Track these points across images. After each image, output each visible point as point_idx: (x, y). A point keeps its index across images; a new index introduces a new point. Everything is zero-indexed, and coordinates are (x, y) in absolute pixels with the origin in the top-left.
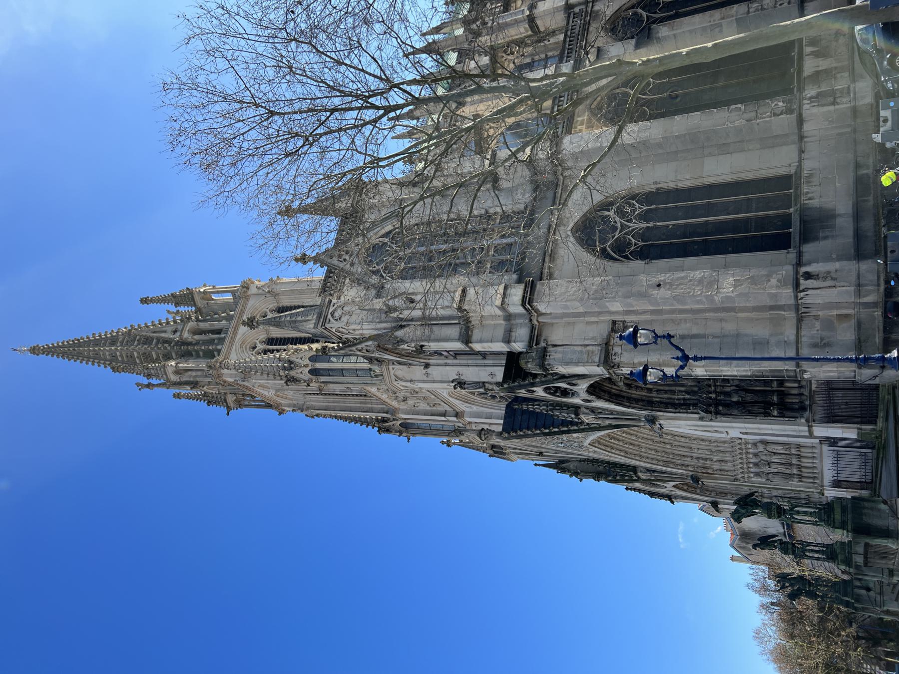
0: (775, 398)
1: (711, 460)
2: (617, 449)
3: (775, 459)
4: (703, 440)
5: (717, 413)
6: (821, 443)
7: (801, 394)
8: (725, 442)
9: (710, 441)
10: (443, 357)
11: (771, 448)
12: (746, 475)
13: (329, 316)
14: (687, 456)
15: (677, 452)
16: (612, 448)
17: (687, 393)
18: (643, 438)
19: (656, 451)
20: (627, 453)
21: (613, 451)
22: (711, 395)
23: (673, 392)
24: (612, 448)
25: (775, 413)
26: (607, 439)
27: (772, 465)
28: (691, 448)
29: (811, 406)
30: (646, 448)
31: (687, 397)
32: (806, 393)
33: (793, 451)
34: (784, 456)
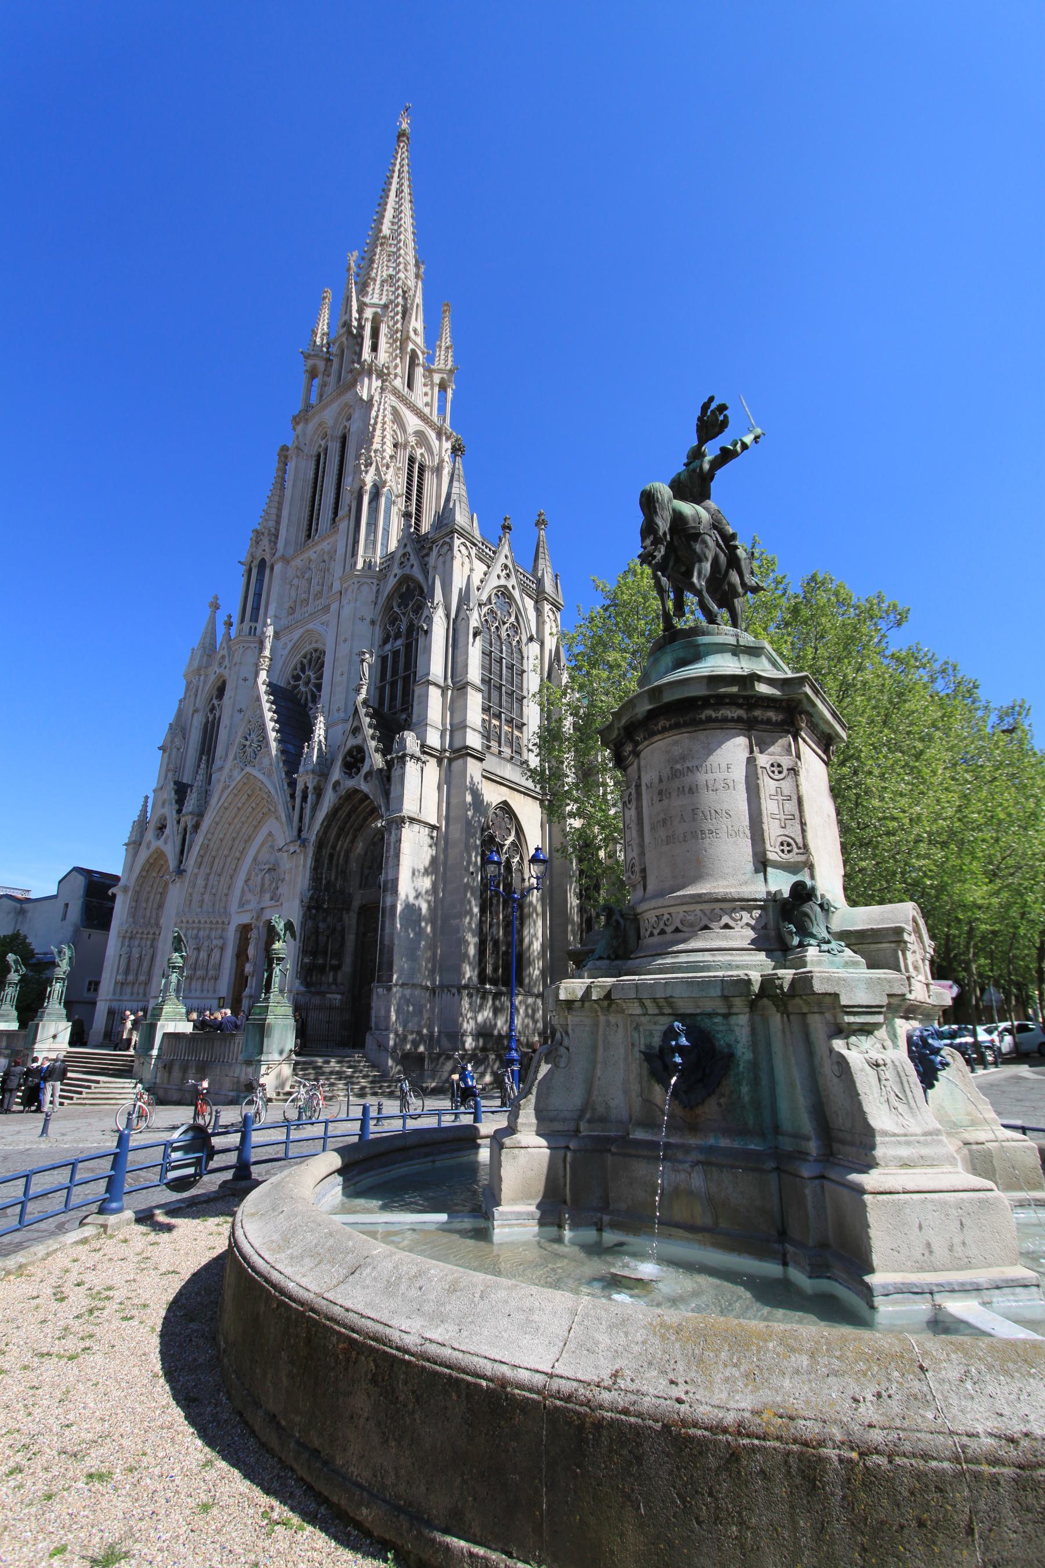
0: (320, 961)
3: (203, 955)
5: (309, 908)
6: (220, 998)
7: (321, 984)
9: (226, 895)
10: (381, 643)
11: (216, 954)
12: (184, 925)
13: (463, 540)
14: (211, 868)
15: (217, 861)
17: (328, 882)
18: (241, 828)
20: (226, 809)
23: (329, 869)
25: (306, 960)
27: (196, 952)
29: (310, 992)
31: (324, 882)
32: (323, 989)
33: (211, 973)
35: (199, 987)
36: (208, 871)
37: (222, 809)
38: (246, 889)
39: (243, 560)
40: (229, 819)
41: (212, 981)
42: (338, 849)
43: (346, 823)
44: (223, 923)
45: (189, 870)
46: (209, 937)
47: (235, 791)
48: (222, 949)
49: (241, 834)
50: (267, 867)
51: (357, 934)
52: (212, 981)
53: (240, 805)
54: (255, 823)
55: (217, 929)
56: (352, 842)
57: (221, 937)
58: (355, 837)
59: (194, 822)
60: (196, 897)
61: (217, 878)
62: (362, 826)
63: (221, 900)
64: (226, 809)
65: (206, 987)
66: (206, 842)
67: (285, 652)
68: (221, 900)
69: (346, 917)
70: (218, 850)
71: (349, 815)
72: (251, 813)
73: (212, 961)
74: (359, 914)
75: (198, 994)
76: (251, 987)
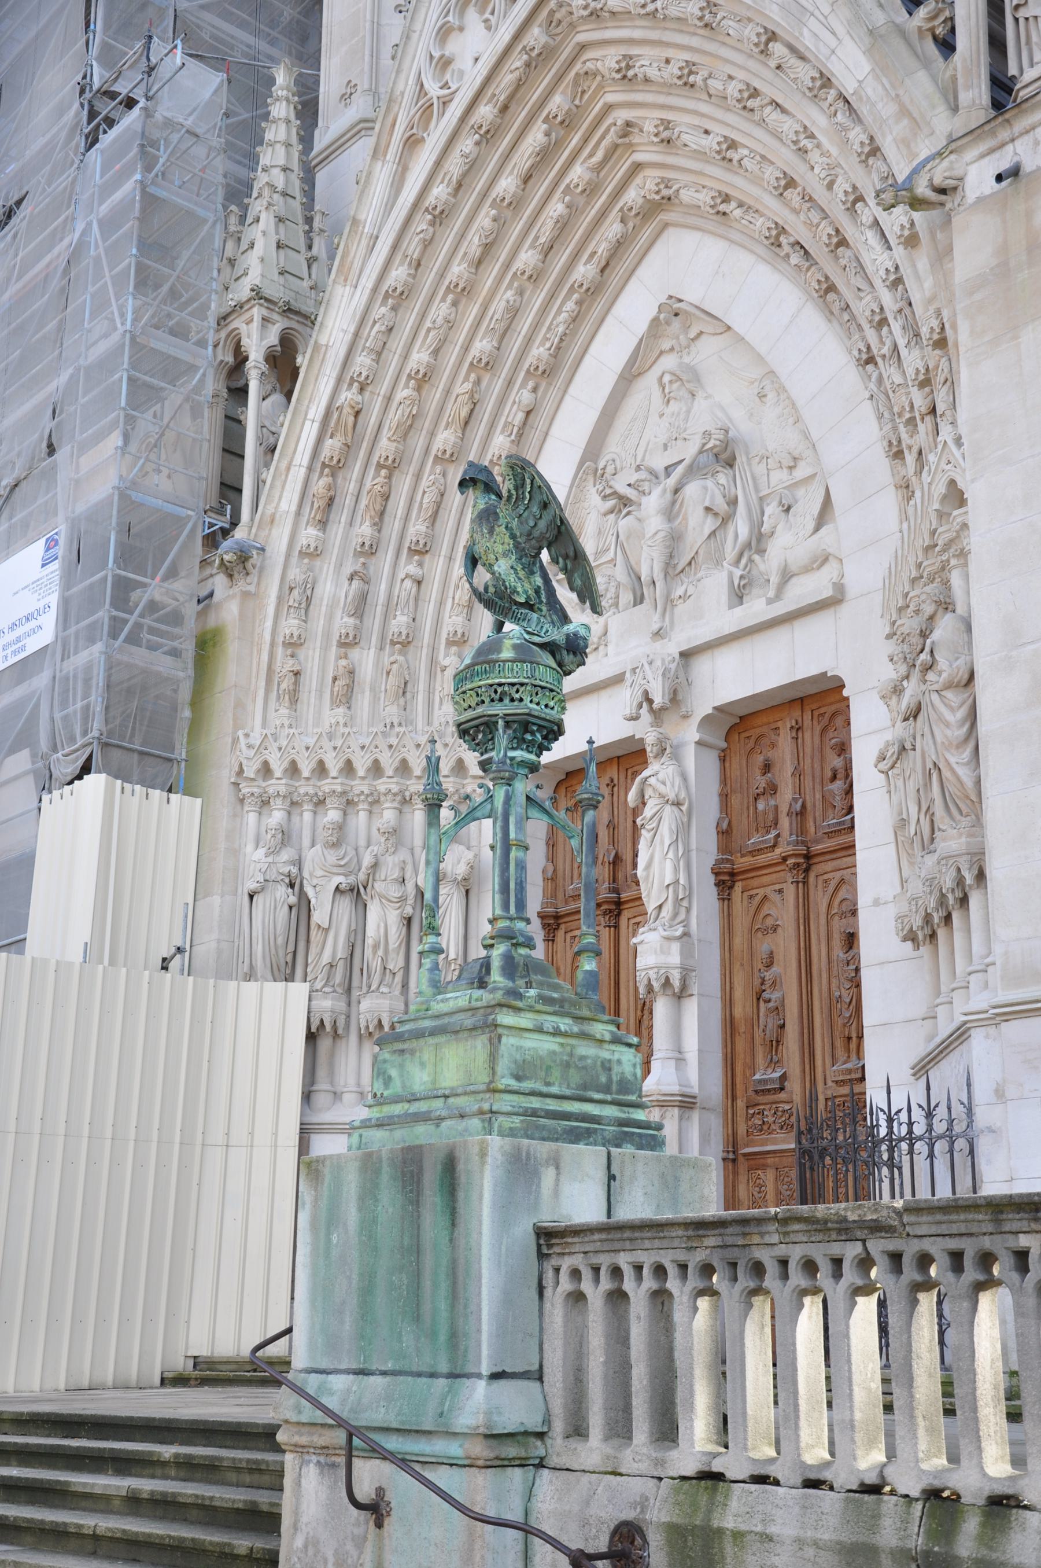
1: (348, 643)
2: (472, 166)
12: (277, 785)
15: (403, 485)
16: (488, 136)
18: (514, 313)
19: (423, 380)
20: (440, 217)
21: (467, 144)
26: (558, 102)
27: (345, 904)
28: (421, 551)
30: (450, 324)
36: (365, 530)
37: (422, 224)
40: (458, 270)
45: (278, 541)
47: (486, 112)
49: (515, 344)
50: (689, 451)
53: (507, 184)
54: (584, 271)
59: (273, 338)
61: (412, 569)
64: (440, 217)
66: (348, 396)
70: (406, 431)
72: (563, 226)
76: (680, 1060)
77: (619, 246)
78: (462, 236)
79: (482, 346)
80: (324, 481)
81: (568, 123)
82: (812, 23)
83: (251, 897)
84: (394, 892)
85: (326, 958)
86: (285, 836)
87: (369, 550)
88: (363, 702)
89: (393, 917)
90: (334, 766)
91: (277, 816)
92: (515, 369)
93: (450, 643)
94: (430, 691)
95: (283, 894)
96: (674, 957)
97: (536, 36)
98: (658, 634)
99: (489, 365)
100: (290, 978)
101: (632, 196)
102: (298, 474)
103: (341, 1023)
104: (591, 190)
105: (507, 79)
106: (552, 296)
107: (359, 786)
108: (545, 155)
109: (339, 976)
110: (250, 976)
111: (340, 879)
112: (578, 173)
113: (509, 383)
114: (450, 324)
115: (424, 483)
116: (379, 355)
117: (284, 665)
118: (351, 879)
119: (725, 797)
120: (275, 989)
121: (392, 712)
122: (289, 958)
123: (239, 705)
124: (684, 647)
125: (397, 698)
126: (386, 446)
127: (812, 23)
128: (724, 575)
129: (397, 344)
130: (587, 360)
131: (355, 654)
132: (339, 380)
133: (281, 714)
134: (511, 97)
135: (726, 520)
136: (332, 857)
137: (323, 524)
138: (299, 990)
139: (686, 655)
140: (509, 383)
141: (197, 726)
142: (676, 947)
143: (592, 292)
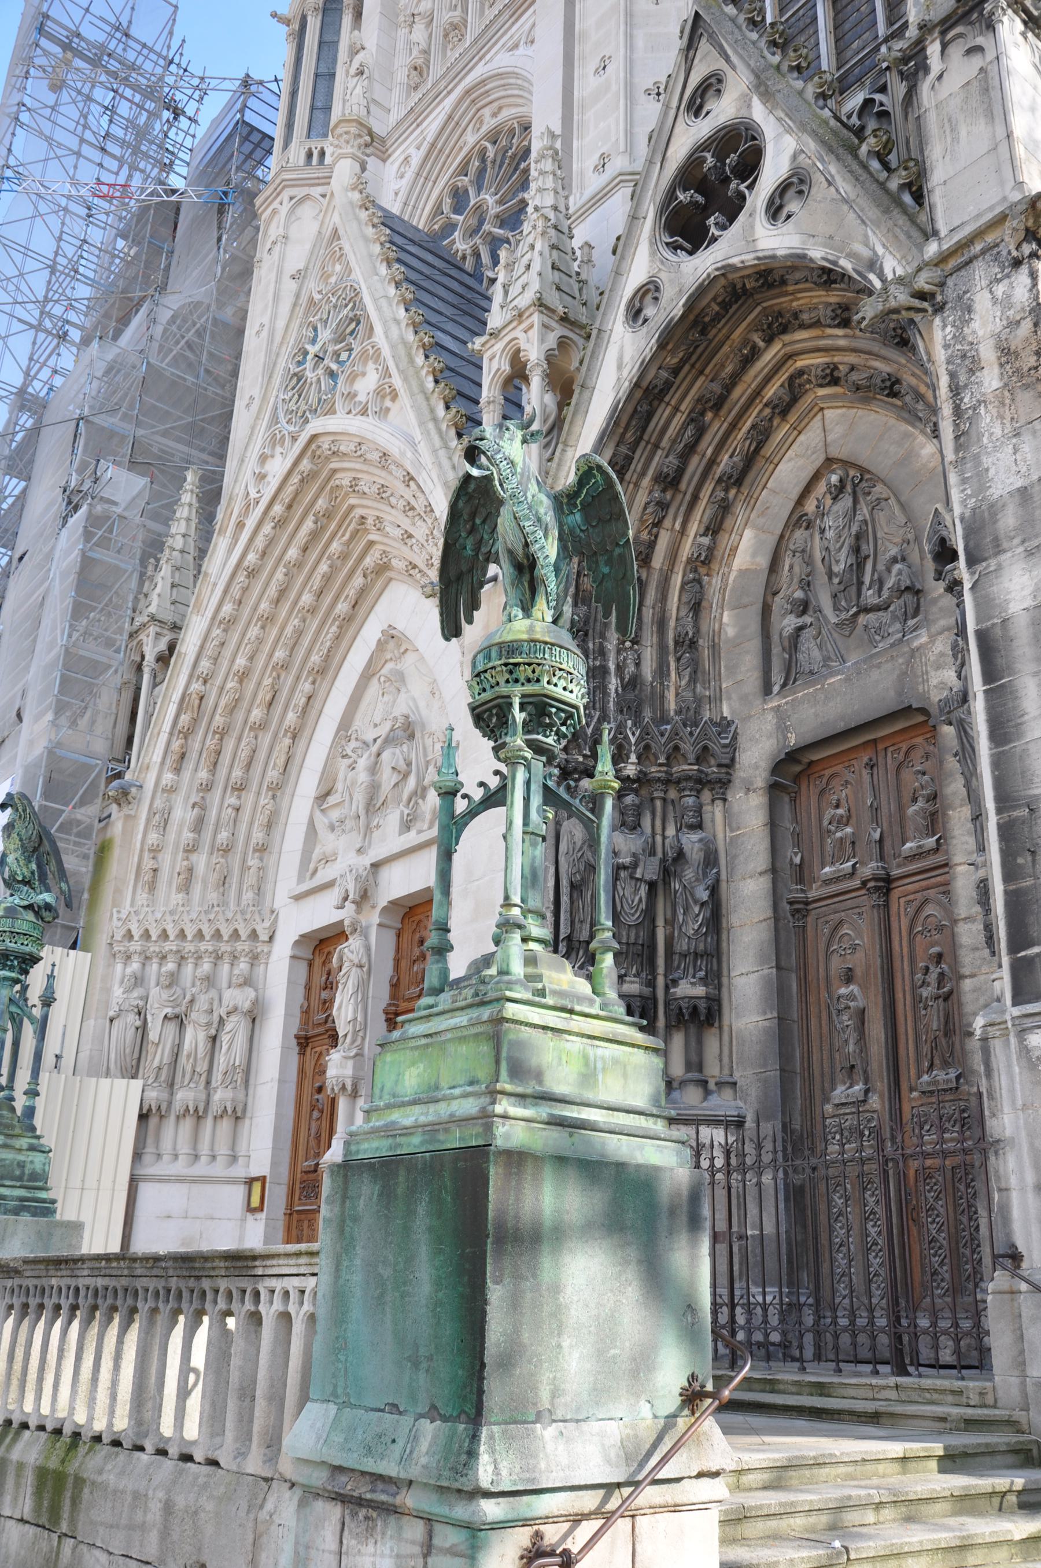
1: (191, 849)
2: (271, 542)
3: (195, 1037)
4: (269, 826)
6: (250, 1182)
8: (259, 891)
9: (262, 849)
11: (235, 1030)
12: (135, 946)
15: (229, 745)
17: (632, 684)
18: (299, 633)
19: (243, 676)
20: (252, 573)
21: (267, 529)
22: (633, 758)
24: (280, 524)
26: (321, 504)
27: (172, 1028)
28: (240, 788)
30: (260, 641)
31: (613, 684)
33: (221, 1096)
34: (202, 1067)
35: (184, 1148)
36: (203, 775)
37: (241, 577)
38: (321, 822)
39: (284, 10)
41: (226, 1124)
42: (658, 561)
43: (685, 456)
44: (254, 935)
46: (209, 981)
47: (278, 509)
48: (254, 1017)
51: (774, 870)
52: (226, 1124)
53: (293, 553)
54: (342, 607)
55: (235, 958)
56: (714, 529)
57: (247, 982)
58: (724, 509)
60: (170, 862)
61: (233, 801)
62: (750, 460)
63: (244, 868)
64: (252, 573)
65: (204, 1149)
66: (196, 686)
67: (405, 183)
68: (244, 868)
69: (715, 813)
70: (232, 709)
71: (697, 425)
72: (328, 579)
73: (222, 1061)
74: (774, 789)
75: (180, 1167)
77: (362, 592)
78: (267, 584)
79: (280, 654)
80: (181, 741)
81: (328, 515)
82: (424, 473)
83: (111, 1021)
84: (203, 1020)
85: (156, 1063)
86: (138, 980)
87: (207, 788)
88: (197, 889)
89: (202, 1036)
90: (172, 934)
91: (135, 966)
92: (301, 670)
93: (255, 851)
94: (241, 882)
95: (132, 1019)
96: (348, 1071)
97: (305, 465)
98: (360, 851)
99: (285, 666)
100: (134, 1077)
101: (369, 561)
102: (164, 737)
103: (164, 1107)
104: (344, 556)
105: (290, 490)
106: (323, 623)
107: (189, 947)
108: (315, 535)
109: (163, 1076)
110: (108, 1074)
111: (168, 1010)
112: (335, 547)
113: (298, 678)
114: (260, 641)
115: (243, 744)
116: (215, 660)
117: (148, 864)
118: (177, 1010)
119: (397, 962)
120: (121, 1083)
121: (213, 896)
122: (134, 1063)
123: (118, 891)
124: (373, 861)
125: (218, 887)
126: (219, 720)
127: (424, 473)
128: (398, 812)
129: (227, 653)
130: (346, 664)
131: (194, 857)
132: (191, 676)
133: (142, 897)
134: (293, 500)
135: (406, 776)
136: (165, 995)
137: (178, 770)
138: (137, 1084)
139: (376, 866)
140: (298, 678)
141: (93, 904)
142: (350, 1064)
143: (348, 620)
